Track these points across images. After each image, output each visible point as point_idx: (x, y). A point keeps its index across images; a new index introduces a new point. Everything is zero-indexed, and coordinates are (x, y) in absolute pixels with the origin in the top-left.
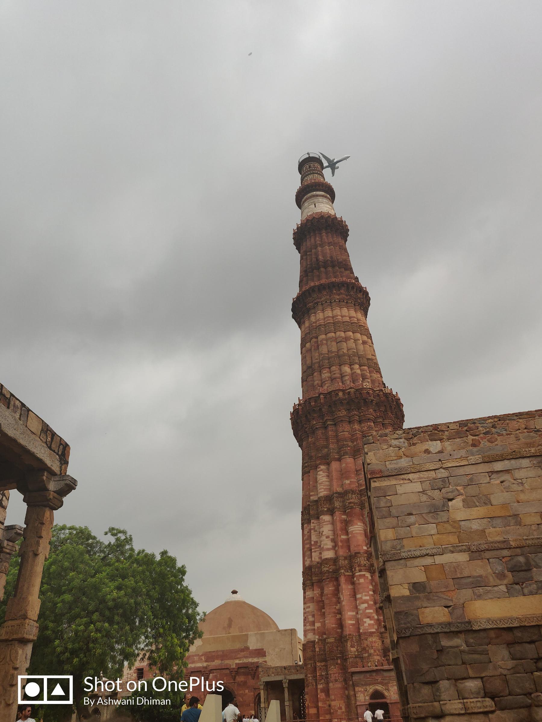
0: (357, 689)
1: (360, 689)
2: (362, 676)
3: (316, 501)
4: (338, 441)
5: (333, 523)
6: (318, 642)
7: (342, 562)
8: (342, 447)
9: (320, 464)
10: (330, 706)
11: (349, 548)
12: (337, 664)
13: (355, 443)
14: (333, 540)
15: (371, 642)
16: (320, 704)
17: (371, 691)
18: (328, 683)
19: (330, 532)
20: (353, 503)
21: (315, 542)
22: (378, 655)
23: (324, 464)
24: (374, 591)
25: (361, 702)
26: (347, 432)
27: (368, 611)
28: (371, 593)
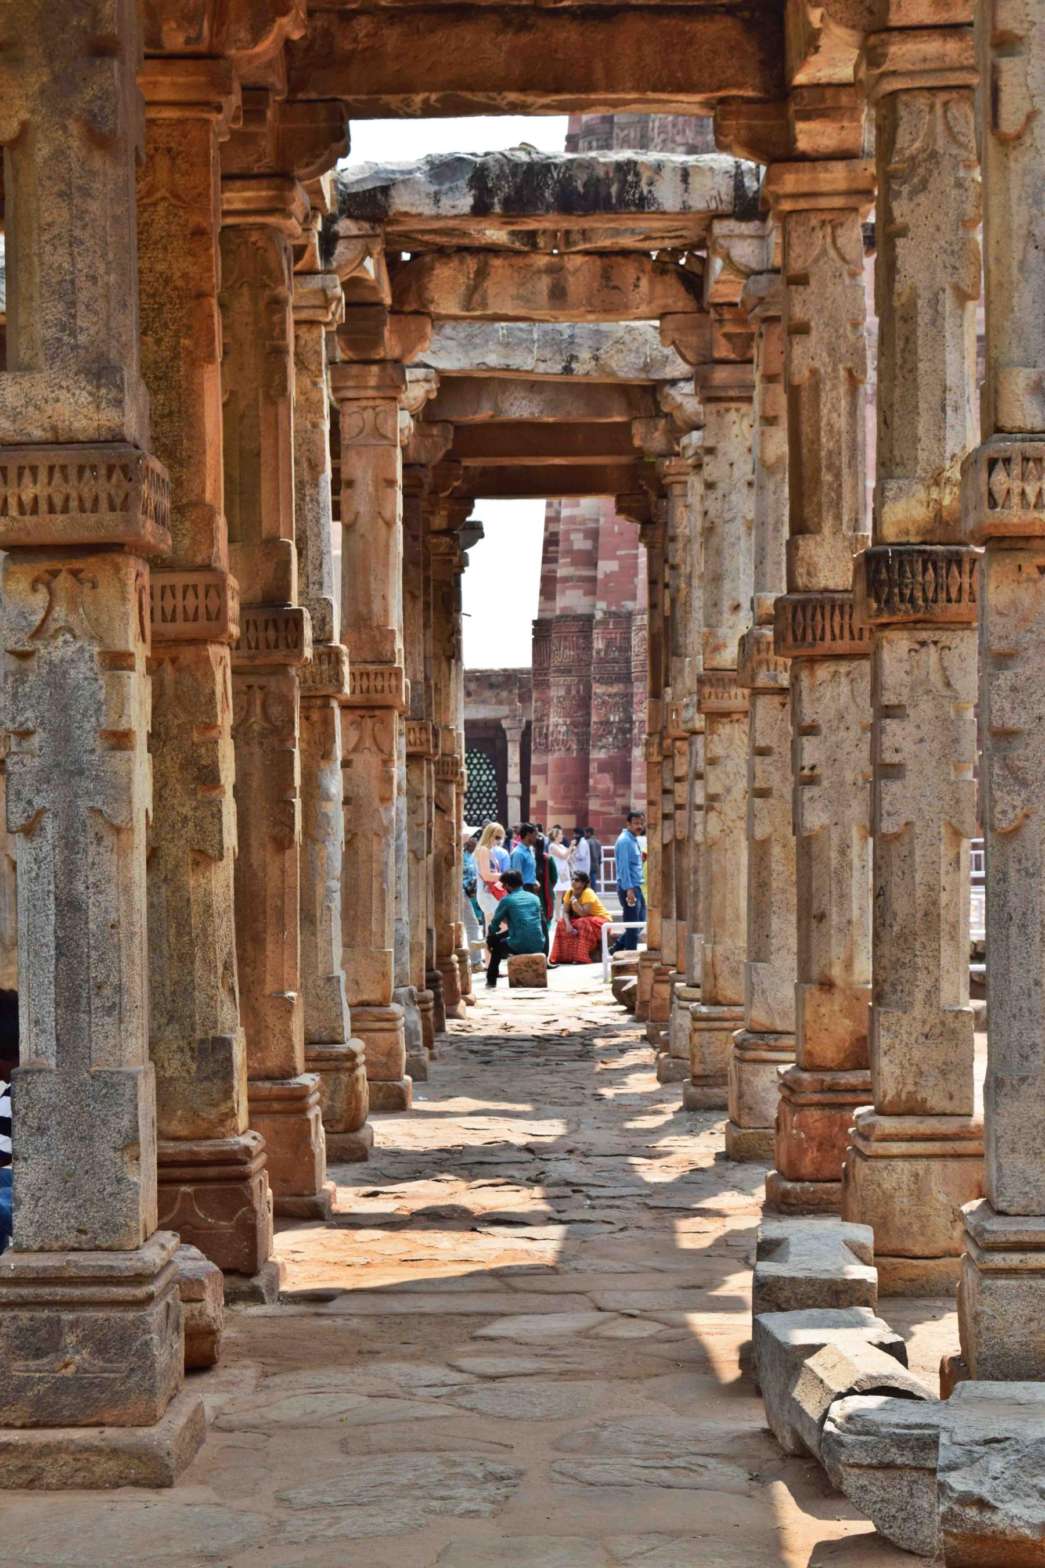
6: (604, 622)
16: (594, 805)
18: (626, 747)
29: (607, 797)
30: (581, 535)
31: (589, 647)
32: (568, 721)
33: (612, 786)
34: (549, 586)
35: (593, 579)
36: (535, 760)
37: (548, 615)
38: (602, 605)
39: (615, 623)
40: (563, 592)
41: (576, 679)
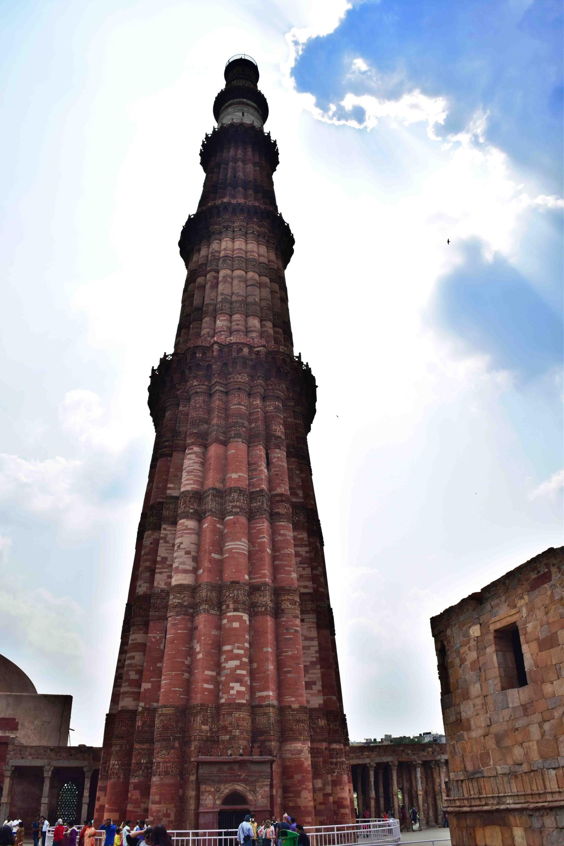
0: (203, 787)
1: (208, 788)
2: (214, 769)
3: (177, 498)
4: (227, 417)
5: (199, 533)
6: (142, 713)
7: (204, 593)
8: (234, 426)
9: (193, 444)
10: (146, 810)
11: (221, 572)
12: (173, 748)
13: (253, 425)
14: (196, 559)
15: (238, 719)
16: (130, 807)
17: (227, 791)
18: (148, 776)
19: (193, 546)
20: (239, 507)
21: (162, 558)
22: (244, 739)
23: (199, 446)
24: (250, 644)
25: (209, 808)
26: (244, 406)
27: (239, 672)
28: (247, 645)
29: (137, 803)
30: (134, 673)
31: (134, 725)
32: (120, 763)
33: (139, 797)
34: (115, 698)
35: (139, 693)
36: (100, 784)
37: (114, 712)
38: (142, 704)
39: (148, 713)
40: (123, 699)
41: (125, 742)
